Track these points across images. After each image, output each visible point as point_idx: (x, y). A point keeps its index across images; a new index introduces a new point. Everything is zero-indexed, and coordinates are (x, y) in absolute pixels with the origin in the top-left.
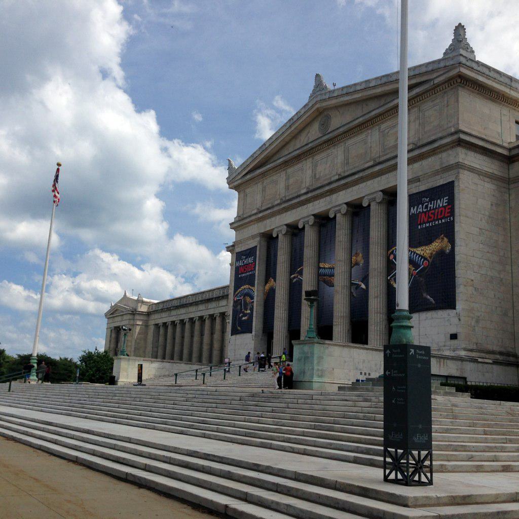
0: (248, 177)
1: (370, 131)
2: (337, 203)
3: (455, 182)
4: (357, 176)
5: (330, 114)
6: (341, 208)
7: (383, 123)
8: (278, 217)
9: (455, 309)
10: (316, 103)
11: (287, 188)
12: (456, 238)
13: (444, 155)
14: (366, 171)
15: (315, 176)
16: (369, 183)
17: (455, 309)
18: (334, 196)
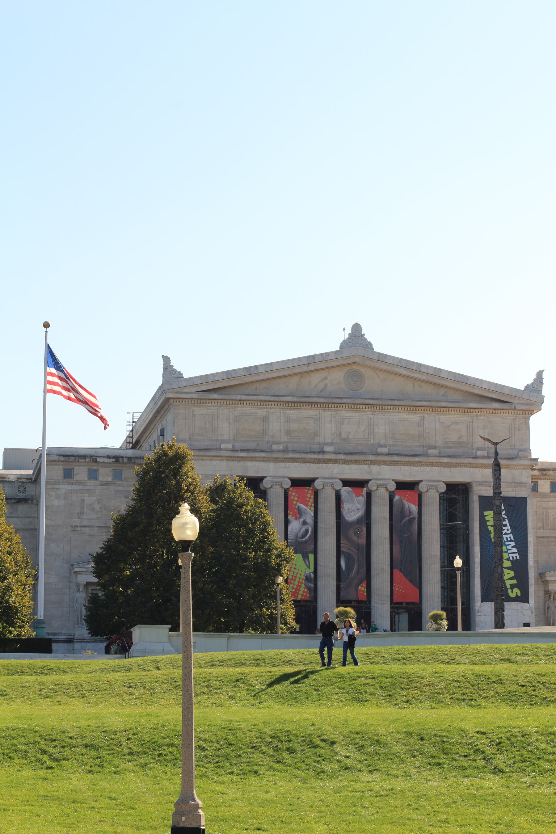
0: (215, 396)
1: (427, 416)
2: (380, 477)
3: (527, 499)
4: (417, 459)
5: (365, 375)
6: (389, 483)
7: (443, 414)
8: (271, 465)
9: (528, 603)
10: (356, 355)
11: (288, 433)
12: (529, 546)
13: (516, 472)
14: (430, 458)
15: (340, 435)
16: (428, 469)
17: (528, 603)
18: (375, 468)
